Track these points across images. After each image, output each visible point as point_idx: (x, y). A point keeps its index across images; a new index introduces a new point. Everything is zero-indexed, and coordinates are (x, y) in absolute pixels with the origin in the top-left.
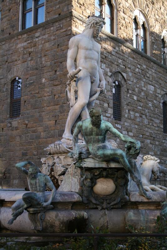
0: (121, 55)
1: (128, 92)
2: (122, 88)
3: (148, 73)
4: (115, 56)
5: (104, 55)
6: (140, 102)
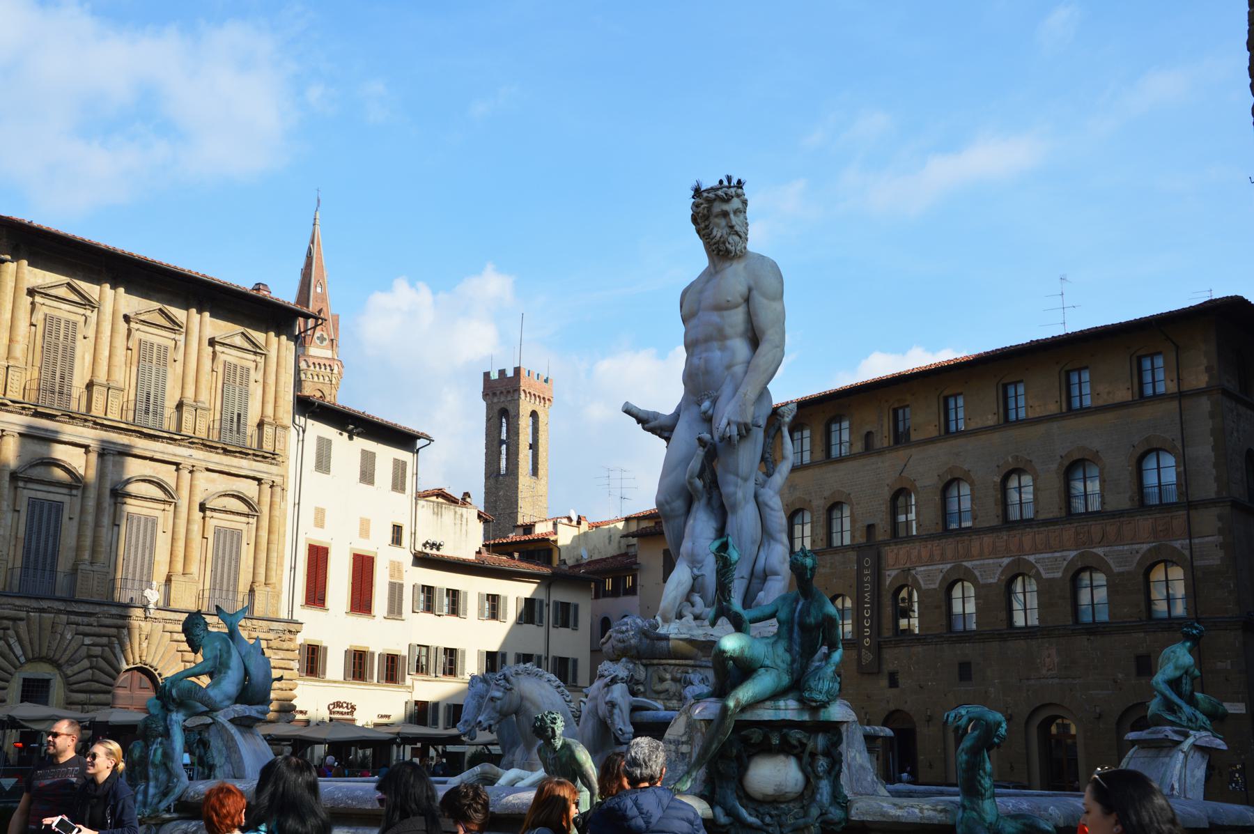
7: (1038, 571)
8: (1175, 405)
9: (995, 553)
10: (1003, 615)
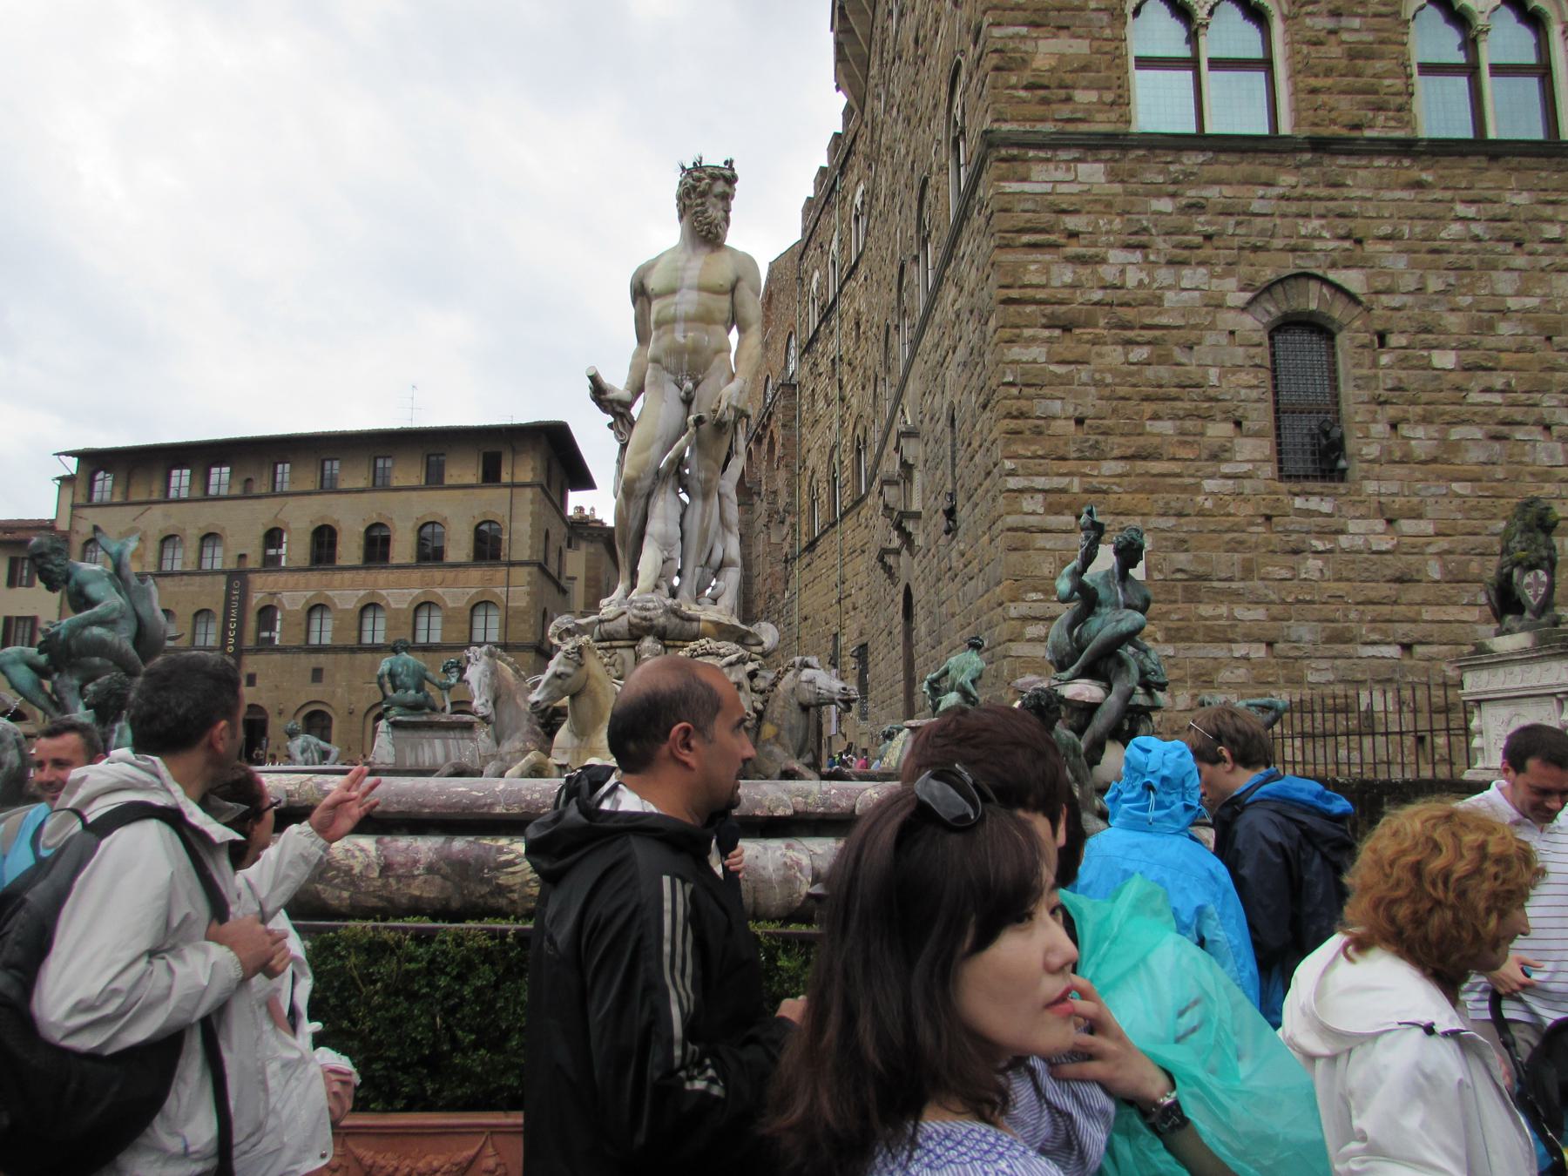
0: (1319, 199)
1: (1382, 343)
2: (1342, 339)
3: (1550, 221)
4: (1272, 215)
5: (1197, 233)
6: (1491, 369)
7: (388, 603)
8: (507, 491)
9: (353, 586)
10: (355, 633)
